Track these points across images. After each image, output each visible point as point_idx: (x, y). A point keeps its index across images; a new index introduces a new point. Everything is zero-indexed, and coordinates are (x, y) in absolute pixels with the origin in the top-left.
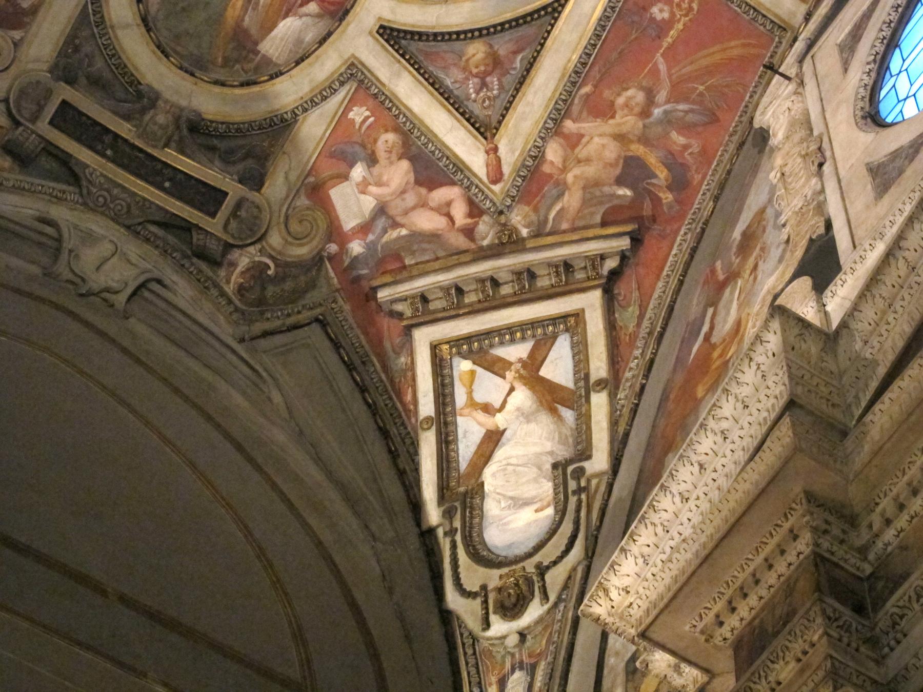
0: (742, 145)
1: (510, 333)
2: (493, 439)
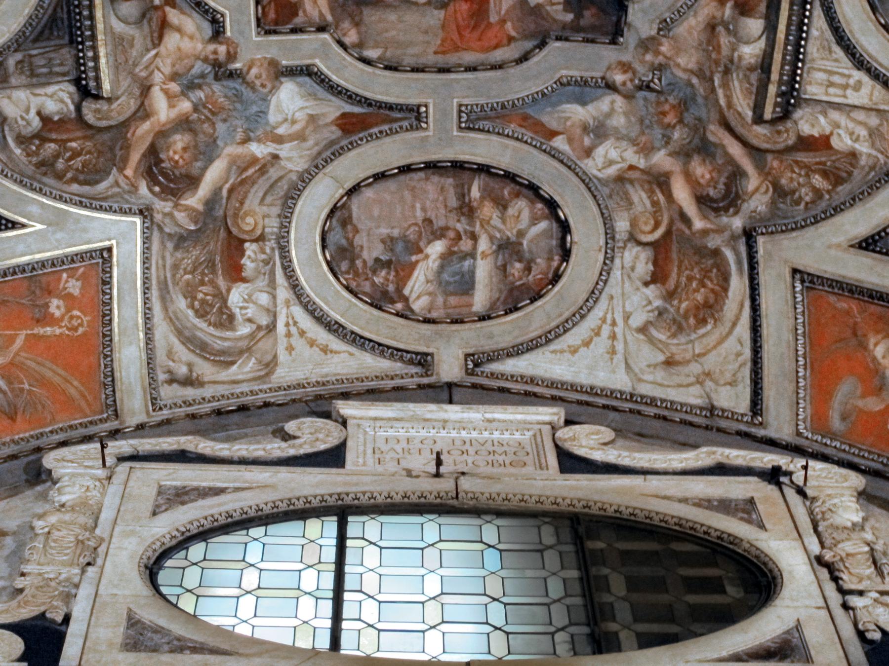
0: (14, 457)
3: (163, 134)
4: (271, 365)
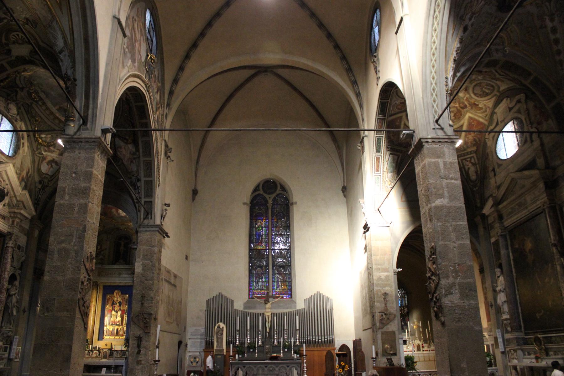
1: (468, 158)
2: (469, 169)
3: (460, 106)
4: (489, 107)
